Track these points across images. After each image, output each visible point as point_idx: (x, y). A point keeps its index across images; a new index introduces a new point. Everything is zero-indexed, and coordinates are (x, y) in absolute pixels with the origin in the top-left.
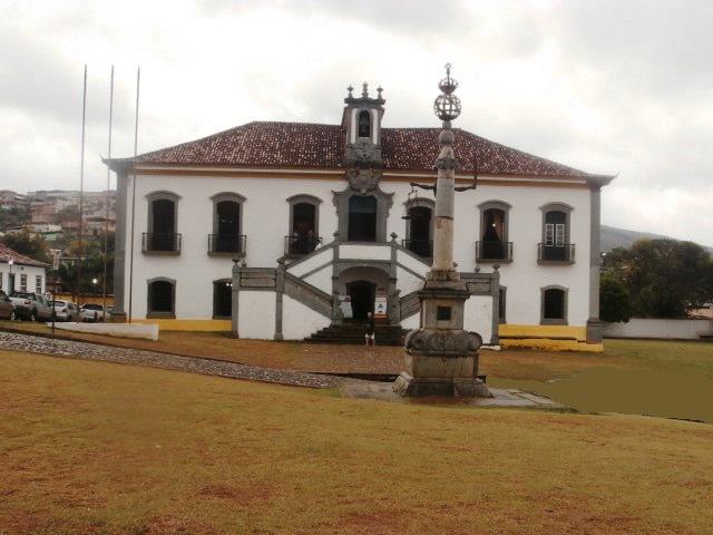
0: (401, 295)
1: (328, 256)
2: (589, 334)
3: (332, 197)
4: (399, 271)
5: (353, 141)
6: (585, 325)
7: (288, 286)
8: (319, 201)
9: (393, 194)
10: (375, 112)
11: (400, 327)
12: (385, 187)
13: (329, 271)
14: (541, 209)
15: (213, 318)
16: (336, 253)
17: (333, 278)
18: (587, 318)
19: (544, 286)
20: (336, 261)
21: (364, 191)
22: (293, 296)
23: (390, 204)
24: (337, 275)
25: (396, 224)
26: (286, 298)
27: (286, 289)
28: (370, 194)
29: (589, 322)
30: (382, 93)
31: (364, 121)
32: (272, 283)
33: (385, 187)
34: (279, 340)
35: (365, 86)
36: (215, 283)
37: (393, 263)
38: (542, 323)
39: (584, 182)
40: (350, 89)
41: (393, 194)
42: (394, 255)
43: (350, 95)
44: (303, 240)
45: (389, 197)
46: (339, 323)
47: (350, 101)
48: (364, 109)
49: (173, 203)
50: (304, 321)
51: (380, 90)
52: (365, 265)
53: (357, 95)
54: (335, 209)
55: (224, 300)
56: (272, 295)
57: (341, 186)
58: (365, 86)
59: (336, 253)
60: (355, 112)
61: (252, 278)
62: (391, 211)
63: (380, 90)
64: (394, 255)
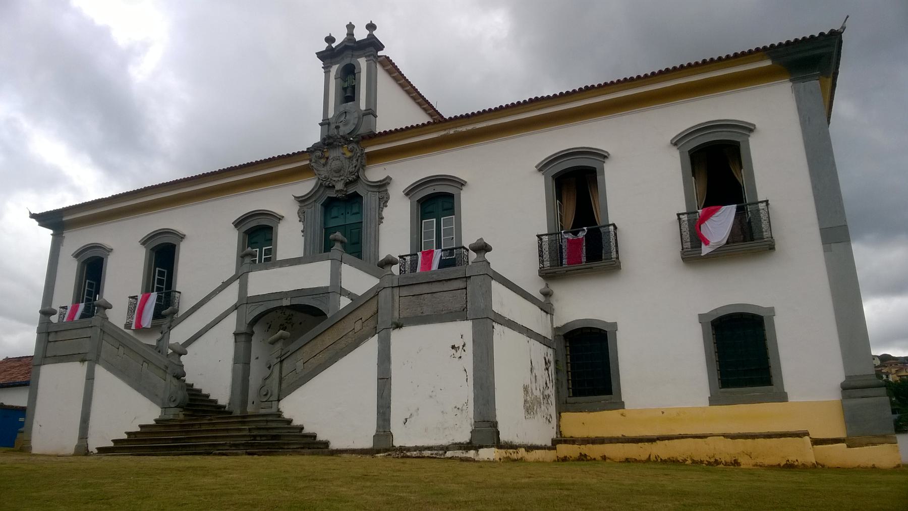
2: (851, 418)
3: (296, 207)
5: (331, 114)
6: (835, 396)
7: (107, 347)
8: (280, 218)
10: (363, 62)
11: (279, 414)
12: (375, 173)
13: (231, 324)
14: (676, 143)
17: (236, 334)
18: (840, 377)
19: (705, 311)
20: (244, 302)
21: (339, 186)
22: (112, 368)
23: (384, 201)
25: (395, 231)
26: (100, 370)
28: (351, 191)
29: (846, 388)
30: (374, 33)
35: (351, 27)
38: (713, 401)
39: (768, 63)
42: (336, 275)
43: (329, 49)
45: (382, 186)
46: (171, 414)
48: (347, 61)
51: (371, 27)
52: (286, 302)
54: (301, 226)
57: (305, 186)
59: (243, 288)
60: (334, 69)
62: (386, 212)
63: (371, 27)
64: (336, 275)
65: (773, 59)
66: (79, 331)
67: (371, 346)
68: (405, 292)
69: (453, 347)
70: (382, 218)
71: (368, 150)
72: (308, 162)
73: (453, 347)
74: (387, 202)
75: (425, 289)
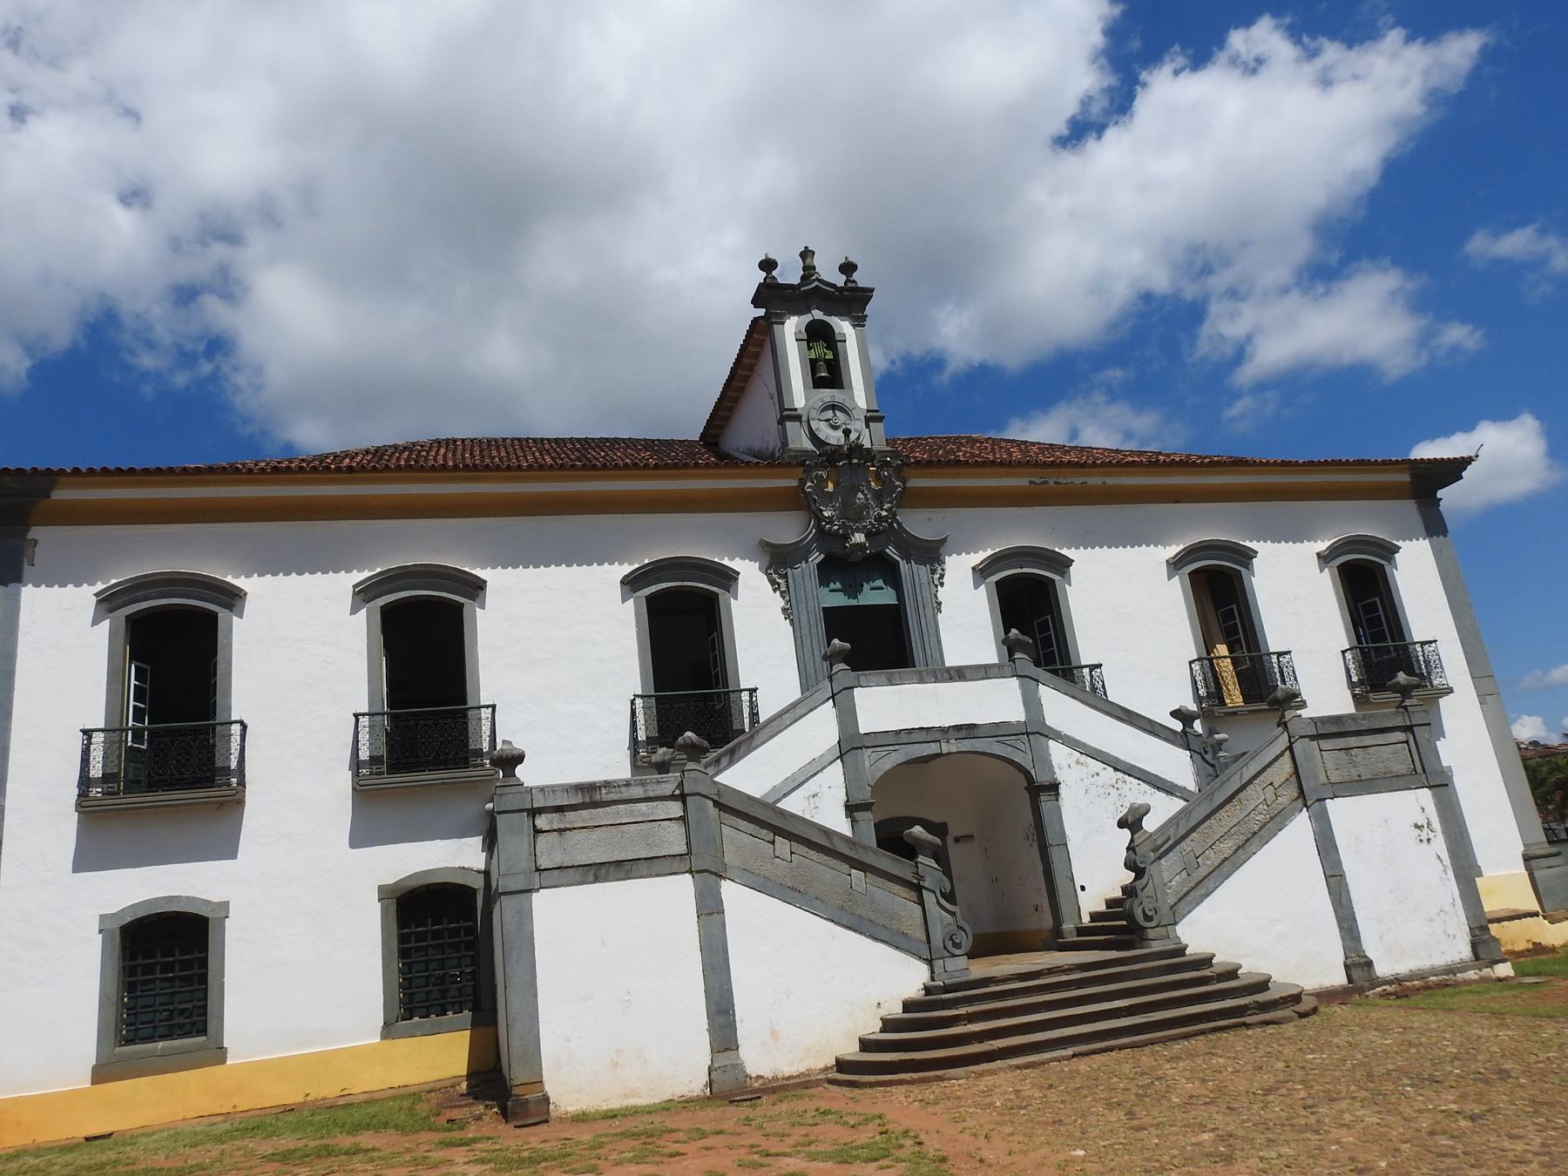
0: (1150, 824)
1: (821, 728)
4: (1057, 751)
7: (737, 840)
9: (944, 540)
12: (919, 524)
15: (388, 1031)
16: (847, 716)
20: (851, 745)
22: (764, 885)
24: (865, 795)
26: (732, 893)
27: (729, 857)
30: (855, 276)
31: (820, 350)
32: (673, 840)
33: (919, 524)
34: (731, 1089)
36: (385, 893)
37: (1035, 730)
40: (768, 265)
41: (944, 540)
42: (1032, 704)
44: (690, 692)
47: (774, 297)
48: (818, 314)
49: (213, 618)
50: (825, 982)
53: (789, 274)
54: (778, 601)
55: (447, 952)
56: (680, 890)
58: (806, 254)
59: (847, 716)
61: (580, 832)
63: (848, 268)
64: (1032, 704)
65: (1413, 476)
66: (643, 806)
67: (1301, 826)
68: (1325, 744)
69: (1416, 826)
70: (940, 604)
71: (914, 483)
72: (794, 483)
73: (1416, 826)
74: (942, 576)
75: (1353, 741)
